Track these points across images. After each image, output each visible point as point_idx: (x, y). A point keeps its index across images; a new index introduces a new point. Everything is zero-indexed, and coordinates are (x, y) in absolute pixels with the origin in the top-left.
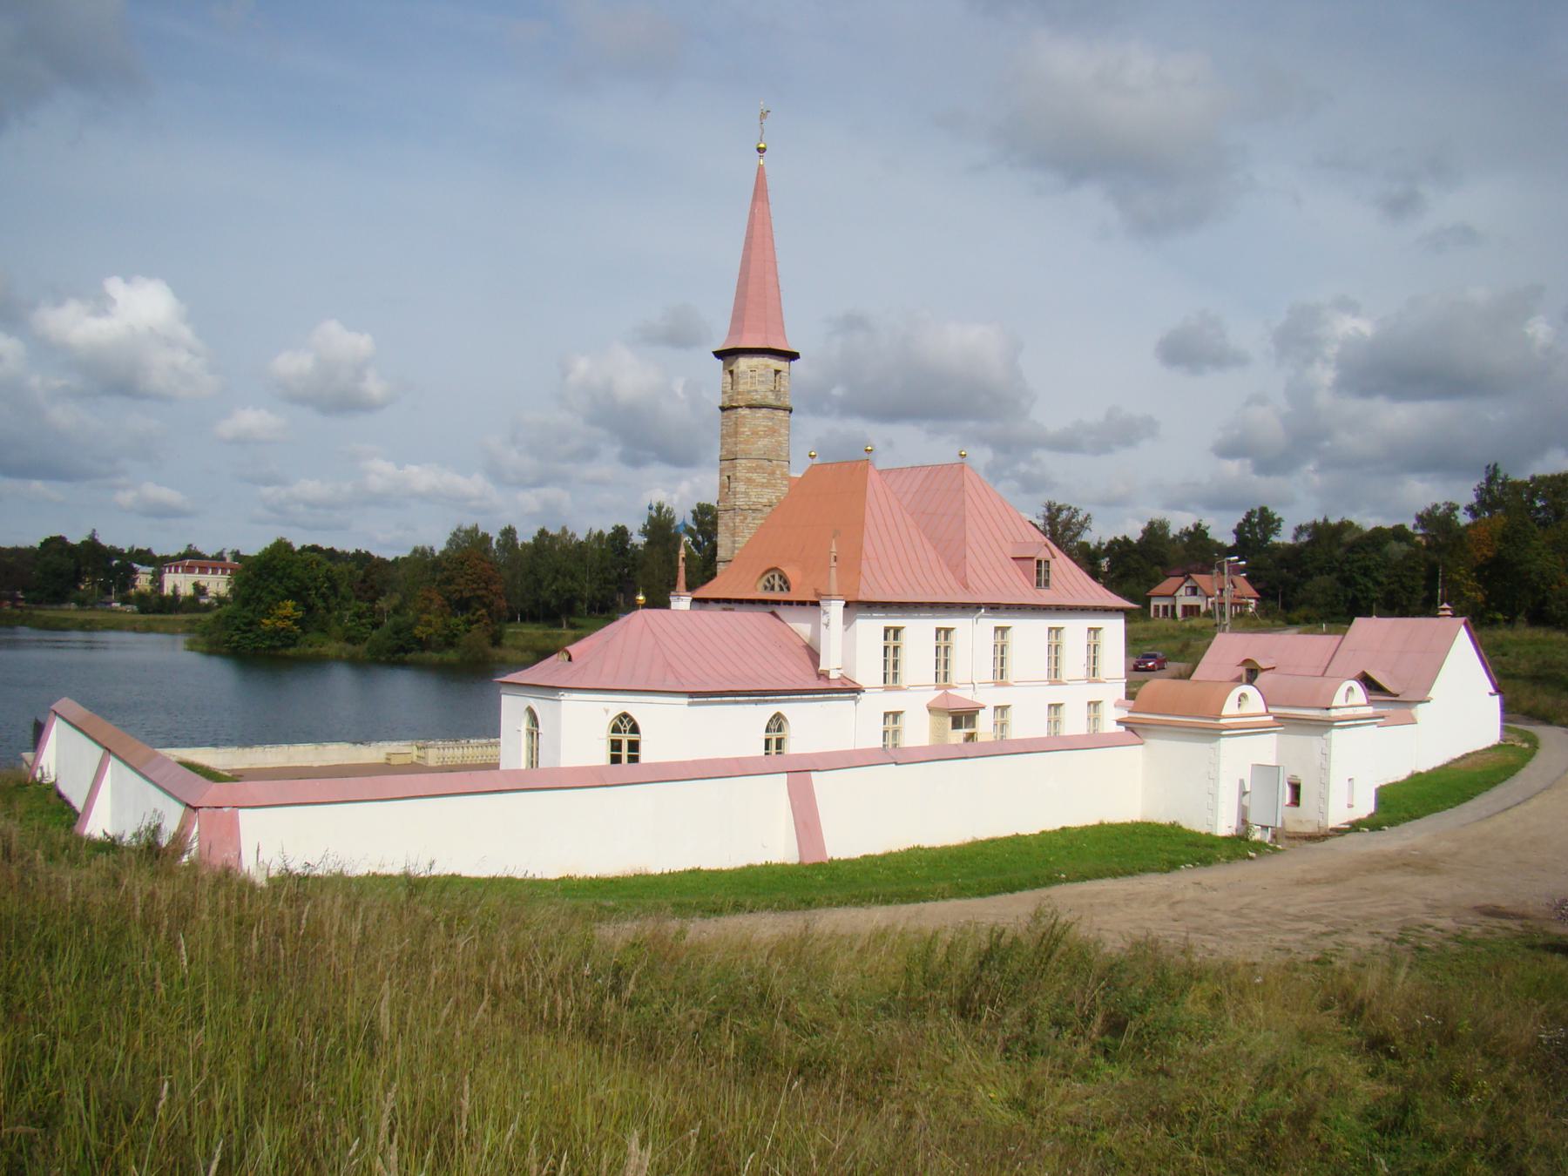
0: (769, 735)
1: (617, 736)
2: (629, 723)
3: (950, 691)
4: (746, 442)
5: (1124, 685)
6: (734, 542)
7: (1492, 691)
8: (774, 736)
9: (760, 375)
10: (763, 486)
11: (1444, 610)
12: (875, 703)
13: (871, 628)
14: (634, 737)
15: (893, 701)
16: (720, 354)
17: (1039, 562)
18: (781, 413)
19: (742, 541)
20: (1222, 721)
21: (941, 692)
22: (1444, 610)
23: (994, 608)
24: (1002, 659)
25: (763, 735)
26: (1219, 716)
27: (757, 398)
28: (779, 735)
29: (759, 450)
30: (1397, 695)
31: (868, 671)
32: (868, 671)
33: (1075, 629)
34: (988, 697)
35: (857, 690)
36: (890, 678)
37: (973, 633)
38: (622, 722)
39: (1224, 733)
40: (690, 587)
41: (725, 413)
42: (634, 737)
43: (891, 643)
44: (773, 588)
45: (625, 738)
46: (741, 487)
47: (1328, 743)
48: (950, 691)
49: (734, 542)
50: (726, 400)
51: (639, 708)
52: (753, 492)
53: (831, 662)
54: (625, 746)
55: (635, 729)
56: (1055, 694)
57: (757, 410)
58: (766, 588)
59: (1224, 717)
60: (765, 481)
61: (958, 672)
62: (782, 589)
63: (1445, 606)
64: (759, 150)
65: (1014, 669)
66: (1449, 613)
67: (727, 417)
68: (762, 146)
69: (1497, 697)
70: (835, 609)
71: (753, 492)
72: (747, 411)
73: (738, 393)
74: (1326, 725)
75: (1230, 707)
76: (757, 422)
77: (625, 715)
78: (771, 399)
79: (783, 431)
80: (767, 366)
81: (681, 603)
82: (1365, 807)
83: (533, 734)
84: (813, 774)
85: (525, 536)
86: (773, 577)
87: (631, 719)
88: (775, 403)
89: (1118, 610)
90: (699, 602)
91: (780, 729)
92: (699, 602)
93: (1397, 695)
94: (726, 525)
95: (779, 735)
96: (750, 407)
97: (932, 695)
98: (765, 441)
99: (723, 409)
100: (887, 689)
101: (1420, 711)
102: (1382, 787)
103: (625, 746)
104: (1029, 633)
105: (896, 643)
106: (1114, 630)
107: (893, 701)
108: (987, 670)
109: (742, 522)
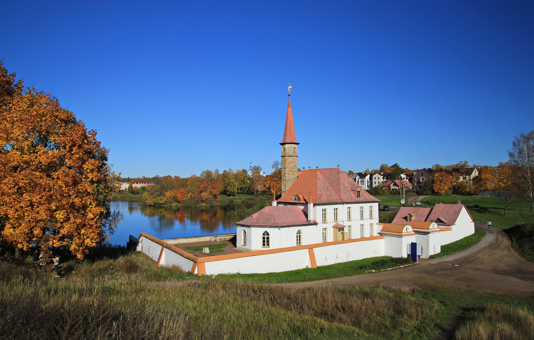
0: (297, 235)
1: (264, 236)
2: (267, 233)
3: (337, 223)
4: (288, 165)
6: (285, 188)
8: (298, 235)
10: (292, 174)
11: (459, 202)
12: (321, 226)
13: (319, 208)
14: (268, 236)
15: (325, 226)
16: (280, 144)
18: (296, 157)
19: (287, 188)
20: (402, 234)
21: (335, 223)
22: (459, 202)
23: (347, 203)
24: (349, 215)
25: (296, 235)
26: (402, 233)
28: (300, 235)
29: (291, 166)
30: (446, 223)
31: (319, 220)
32: (319, 220)
33: (366, 206)
34: (346, 224)
36: (324, 220)
37: (342, 209)
38: (265, 233)
39: (403, 237)
40: (276, 199)
41: (283, 158)
42: (268, 236)
44: (296, 200)
45: (266, 236)
46: (287, 175)
47: (428, 237)
48: (337, 223)
49: (285, 188)
50: (283, 155)
51: (269, 230)
52: (290, 176)
53: (311, 218)
54: (266, 238)
55: (268, 234)
56: (362, 222)
57: (290, 157)
58: (294, 199)
59: (403, 233)
61: (340, 218)
62: (298, 200)
63: (459, 201)
64: (289, 95)
65: (352, 217)
66: (460, 202)
67: (283, 159)
71: (290, 176)
72: (288, 157)
73: (286, 153)
74: (428, 233)
75: (404, 231)
77: (266, 231)
78: (293, 154)
79: (296, 162)
80: (292, 147)
81: (275, 203)
82: (438, 251)
83: (245, 236)
84: (313, 248)
85: (221, 172)
86: (296, 197)
87: (267, 232)
90: (278, 203)
91: (300, 233)
92: (278, 203)
93: (446, 223)
94: (284, 184)
95: (300, 235)
97: (334, 224)
98: (292, 164)
99: (282, 157)
100: (323, 223)
101: (453, 227)
102: (442, 246)
103: (266, 238)
104: (355, 208)
105: (325, 212)
106: (376, 206)
107: (325, 226)
108: (346, 217)
109: (287, 183)
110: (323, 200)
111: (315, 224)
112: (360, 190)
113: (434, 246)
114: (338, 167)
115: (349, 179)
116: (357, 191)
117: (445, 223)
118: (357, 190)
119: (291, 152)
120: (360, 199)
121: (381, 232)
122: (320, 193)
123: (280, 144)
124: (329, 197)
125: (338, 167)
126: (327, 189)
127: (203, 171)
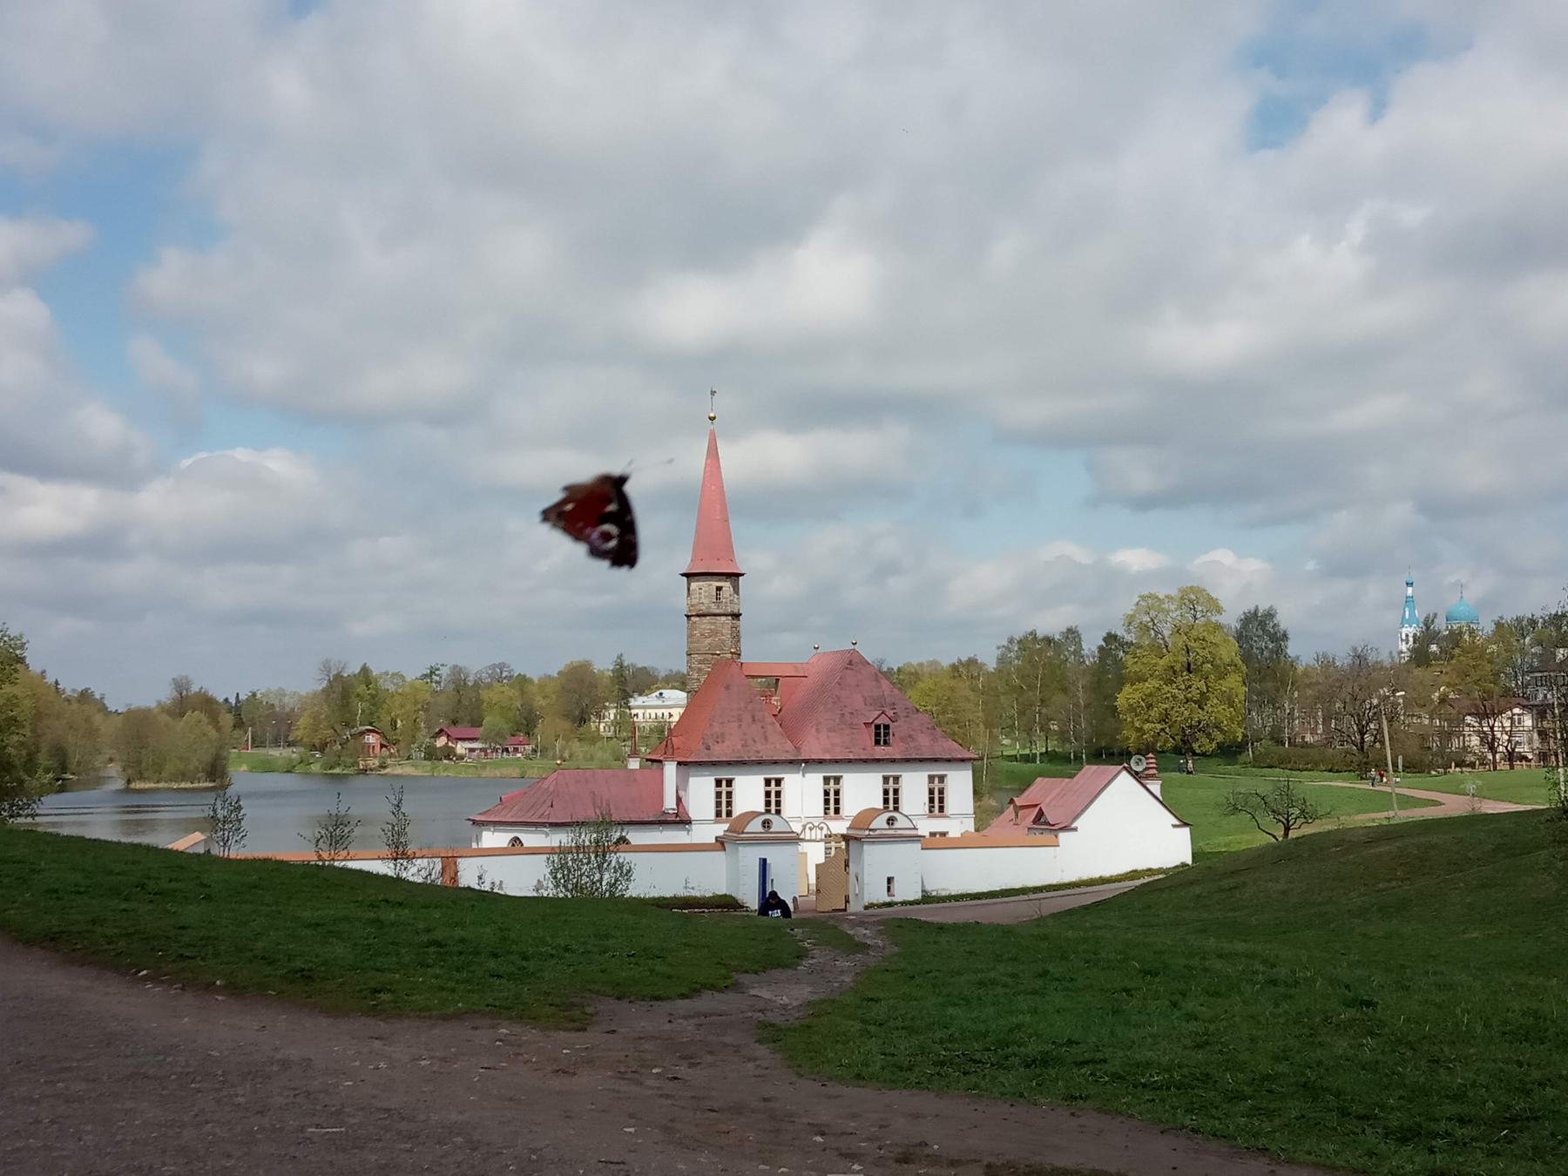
5: (973, 819)
7: (1177, 823)
9: (705, 591)
16: (683, 575)
17: (878, 727)
27: (704, 609)
30: (1053, 825)
35: (689, 822)
43: (724, 788)
60: (710, 670)
68: (712, 415)
69: (1187, 830)
70: (670, 769)
72: (697, 619)
76: (704, 626)
77: (518, 839)
84: (459, 860)
87: (520, 842)
88: (718, 611)
89: (963, 760)
93: (1053, 825)
96: (698, 616)
98: (709, 640)
99: (688, 616)
101: (1063, 837)
110: (719, 753)
111: (681, 820)
112: (887, 721)
113: (890, 880)
114: (853, 647)
115: (880, 687)
116: (878, 727)
117: (1048, 824)
118: (877, 722)
119: (706, 601)
120: (880, 752)
121: (727, 833)
122: (717, 729)
123: (683, 575)
124: (750, 742)
125: (853, 647)
126: (753, 717)
127: (1011, 641)
